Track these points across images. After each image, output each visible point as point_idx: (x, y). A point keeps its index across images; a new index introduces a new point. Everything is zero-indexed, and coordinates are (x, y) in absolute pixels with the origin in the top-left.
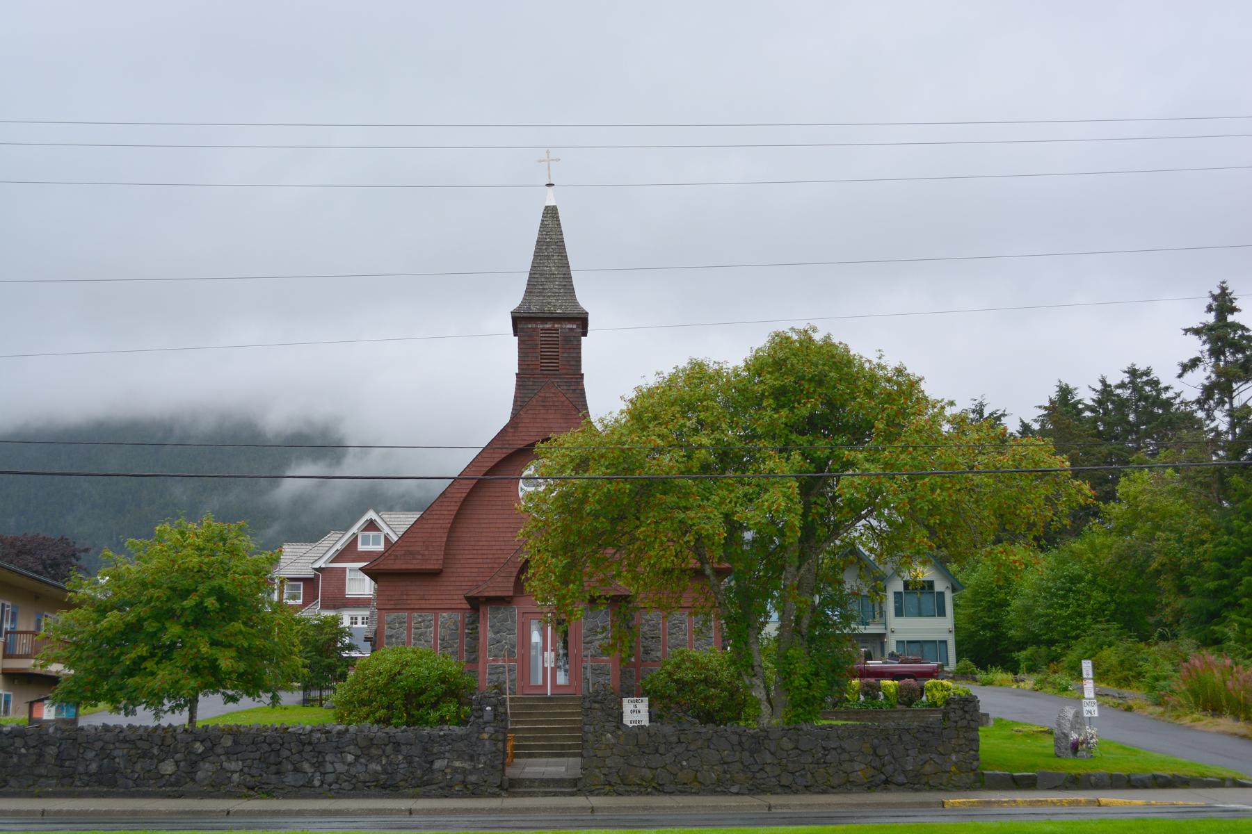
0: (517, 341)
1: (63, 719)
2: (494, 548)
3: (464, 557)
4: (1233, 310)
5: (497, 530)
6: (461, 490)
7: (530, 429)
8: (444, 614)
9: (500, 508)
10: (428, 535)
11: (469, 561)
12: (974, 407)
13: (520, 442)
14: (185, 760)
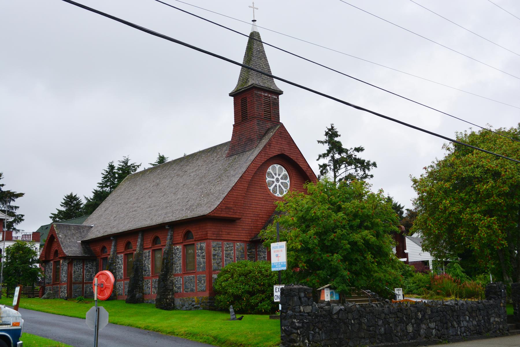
1: (334, 300)
2: (258, 209)
3: (245, 212)
5: (258, 199)
6: (249, 176)
7: (276, 148)
8: (238, 244)
9: (259, 187)
10: (235, 199)
11: (248, 215)
12: (124, 160)
13: (272, 154)
14: (416, 323)
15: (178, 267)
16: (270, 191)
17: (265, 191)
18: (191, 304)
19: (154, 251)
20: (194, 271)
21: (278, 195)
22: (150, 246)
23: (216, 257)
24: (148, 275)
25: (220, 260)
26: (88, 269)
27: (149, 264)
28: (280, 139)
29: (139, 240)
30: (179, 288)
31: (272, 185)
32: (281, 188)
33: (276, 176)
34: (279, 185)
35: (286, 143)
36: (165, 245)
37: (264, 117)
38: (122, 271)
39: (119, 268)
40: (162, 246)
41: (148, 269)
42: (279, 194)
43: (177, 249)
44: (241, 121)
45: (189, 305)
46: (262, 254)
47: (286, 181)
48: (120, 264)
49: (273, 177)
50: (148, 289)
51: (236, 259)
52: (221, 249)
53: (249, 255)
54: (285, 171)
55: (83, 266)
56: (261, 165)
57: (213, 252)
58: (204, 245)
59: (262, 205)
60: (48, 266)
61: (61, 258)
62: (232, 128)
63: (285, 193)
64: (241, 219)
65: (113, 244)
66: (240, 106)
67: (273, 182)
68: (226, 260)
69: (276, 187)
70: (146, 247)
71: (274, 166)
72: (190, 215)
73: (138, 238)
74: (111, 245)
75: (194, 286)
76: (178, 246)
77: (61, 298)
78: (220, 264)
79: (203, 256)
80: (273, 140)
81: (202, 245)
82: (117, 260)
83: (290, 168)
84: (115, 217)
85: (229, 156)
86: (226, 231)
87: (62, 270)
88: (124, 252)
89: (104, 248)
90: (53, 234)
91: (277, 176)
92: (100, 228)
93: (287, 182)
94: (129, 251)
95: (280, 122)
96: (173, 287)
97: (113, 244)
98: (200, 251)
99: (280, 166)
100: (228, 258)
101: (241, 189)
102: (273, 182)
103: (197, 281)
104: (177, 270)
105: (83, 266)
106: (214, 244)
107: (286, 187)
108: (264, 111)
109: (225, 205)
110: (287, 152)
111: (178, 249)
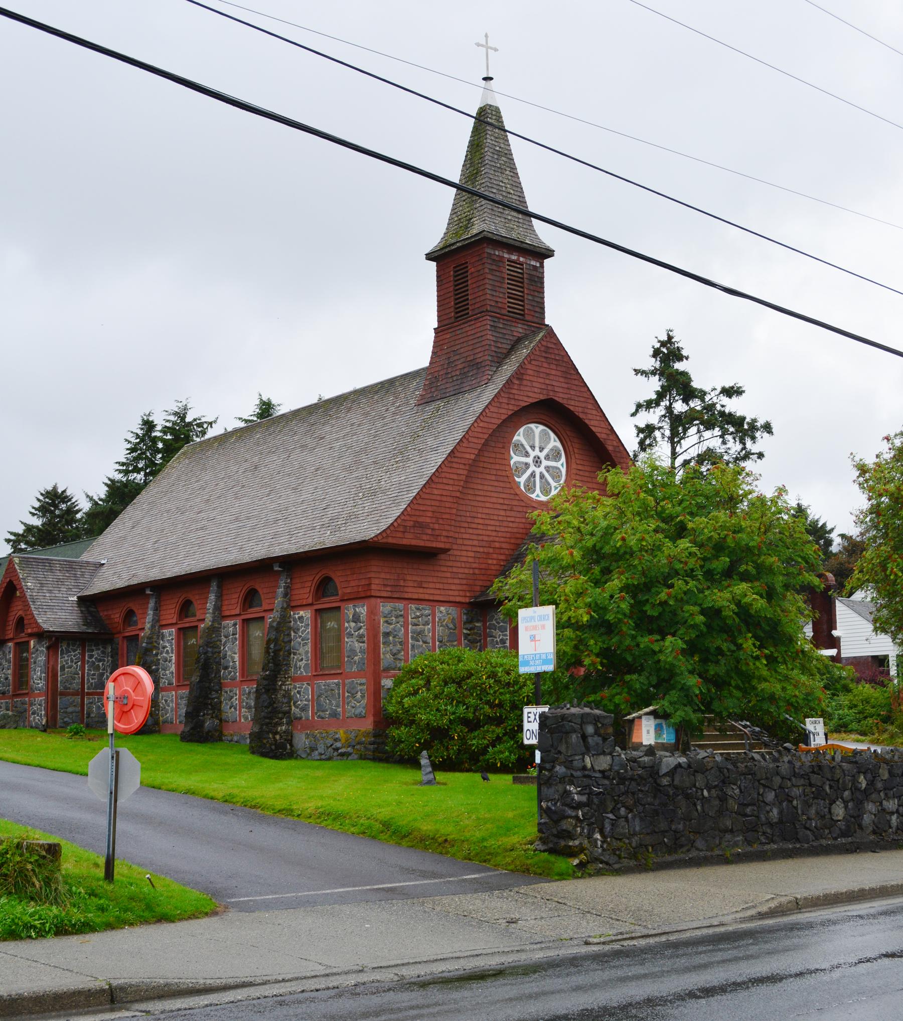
0: (435, 268)
1: (662, 744)
2: (490, 528)
3: (460, 535)
4: (680, 358)
5: (491, 506)
6: (469, 450)
7: (535, 384)
8: (442, 609)
9: (493, 478)
10: (437, 504)
11: (466, 542)
12: (176, 409)
13: (526, 399)
14: (852, 800)
15: (302, 660)
16: (519, 487)
17: (508, 485)
18: (331, 745)
19: (246, 622)
20: (339, 671)
21: (538, 496)
22: (237, 611)
23: (391, 638)
24: (233, 679)
25: (399, 647)
26: (93, 663)
27: (235, 653)
28: (545, 365)
29: (212, 597)
30: (304, 709)
31: (525, 472)
32: (546, 480)
33: (534, 450)
35: (559, 373)
37: (509, 312)
38: (173, 668)
39: (166, 660)
40: (265, 611)
41: (231, 664)
42: (540, 494)
43: (299, 618)
44: (453, 320)
45: (328, 748)
46: (497, 633)
47: (558, 464)
48: (167, 651)
49: (527, 455)
50: (233, 709)
52: (402, 619)
53: (466, 635)
56: (499, 426)
57: (383, 628)
58: (363, 610)
59: (500, 518)
61: (31, 635)
62: (432, 335)
63: (554, 492)
64: (451, 552)
65: (152, 604)
66: (452, 284)
67: (527, 465)
68: (413, 646)
69: (534, 477)
70: (227, 613)
72: (329, 539)
73: (209, 593)
74: (147, 608)
75: (338, 706)
76: (302, 613)
78: (399, 656)
79: (361, 636)
80: (529, 366)
81: (357, 609)
83: (568, 433)
84: (156, 542)
85: (424, 401)
86: (415, 578)
87: (35, 663)
88: (176, 624)
89: (130, 614)
90: (13, 579)
91: (537, 452)
92: (120, 567)
94: (187, 622)
95: (547, 323)
96: (290, 706)
97: (152, 604)
98: (353, 624)
99: (544, 428)
100: (418, 641)
101: (451, 482)
102: (527, 465)
103: (347, 694)
104: (300, 668)
106: (385, 608)
107: (556, 477)
108: (509, 297)
109: (414, 519)
110: (561, 395)
111: (301, 618)
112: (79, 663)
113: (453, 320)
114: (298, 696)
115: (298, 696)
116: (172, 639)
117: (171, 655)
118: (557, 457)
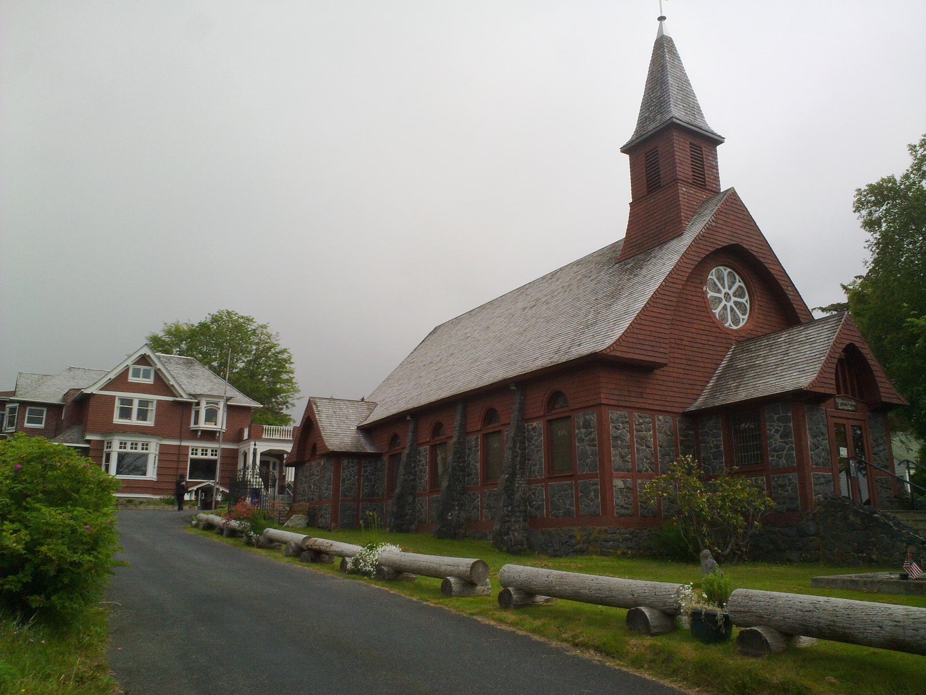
8: (661, 417)
15: (536, 465)
16: (715, 317)
17: (706, 314)
18: (566, 542)
19: (486, 436)
26: (367, 476)
29: (458, 418)
30: (539, 508)
34: (731, 306)
36: (509, 424)
37: (694, 182)
39: (421, 471)
44: (646, 193)
45: (563, 544)
47: (743, 301)
49: (719, 291)
50: (475, 510)
51: (658, 448)
52: (627, 425)
54: (739, 282)
55: (360, 471)
56: (700, 262)
57: (612, 432)
58: (593, 418)
59: (703, 342)
60: (301, 472)
63: (742, 324)
64: (665, 368)
67: (720, 300)
68: (638, 449)
71: (718, 269)
76: (535, 424)
77: (319, 528)
82: (418, 457)
89: (395, 437)
90: (310, 414)
91: (727, 290)
93: (745, 303)
96: (526, 506)
97: (411, 426)
98: (583, 430)
99: (730, 270)
103: (580, 494)
104: (534, 472)
105: (360, 471)
111: (534, 429)
112: (356, 477)
113: (646, 193)
114: (533, 497)
115: (533, 497)
116: (427, 454)
117: (425, 467)
118: (741, 296)
